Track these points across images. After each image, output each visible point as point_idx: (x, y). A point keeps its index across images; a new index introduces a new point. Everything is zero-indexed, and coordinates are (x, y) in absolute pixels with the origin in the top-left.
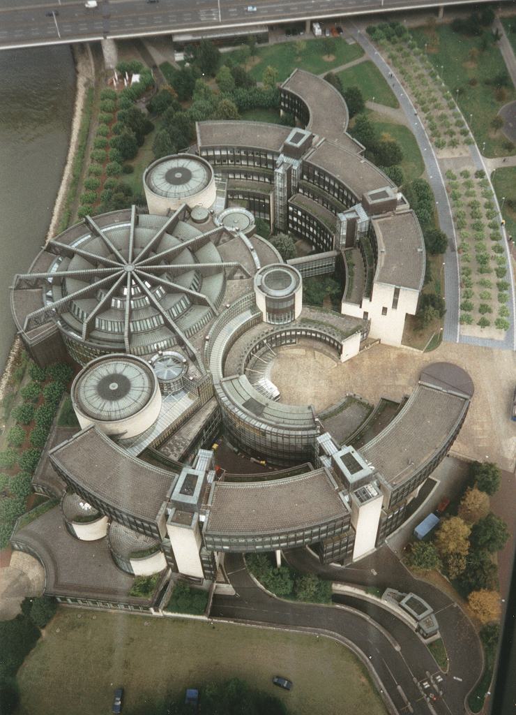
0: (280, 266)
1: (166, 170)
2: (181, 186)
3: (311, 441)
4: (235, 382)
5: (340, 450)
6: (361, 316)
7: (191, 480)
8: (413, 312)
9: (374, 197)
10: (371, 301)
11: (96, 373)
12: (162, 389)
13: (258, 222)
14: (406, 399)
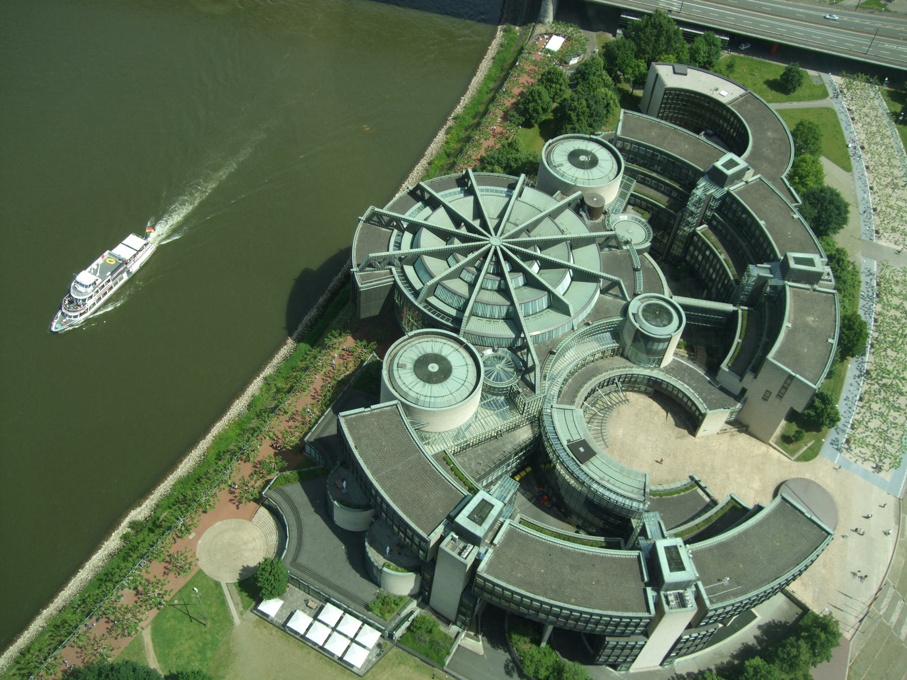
1: (572, 149)
2: (582, 171)
4: (568, 413)
5: (664, 537)
7: (484, 508)
9: (798, 261)
10: (755, 377)
13: (654, 240)
14: (759, 508)
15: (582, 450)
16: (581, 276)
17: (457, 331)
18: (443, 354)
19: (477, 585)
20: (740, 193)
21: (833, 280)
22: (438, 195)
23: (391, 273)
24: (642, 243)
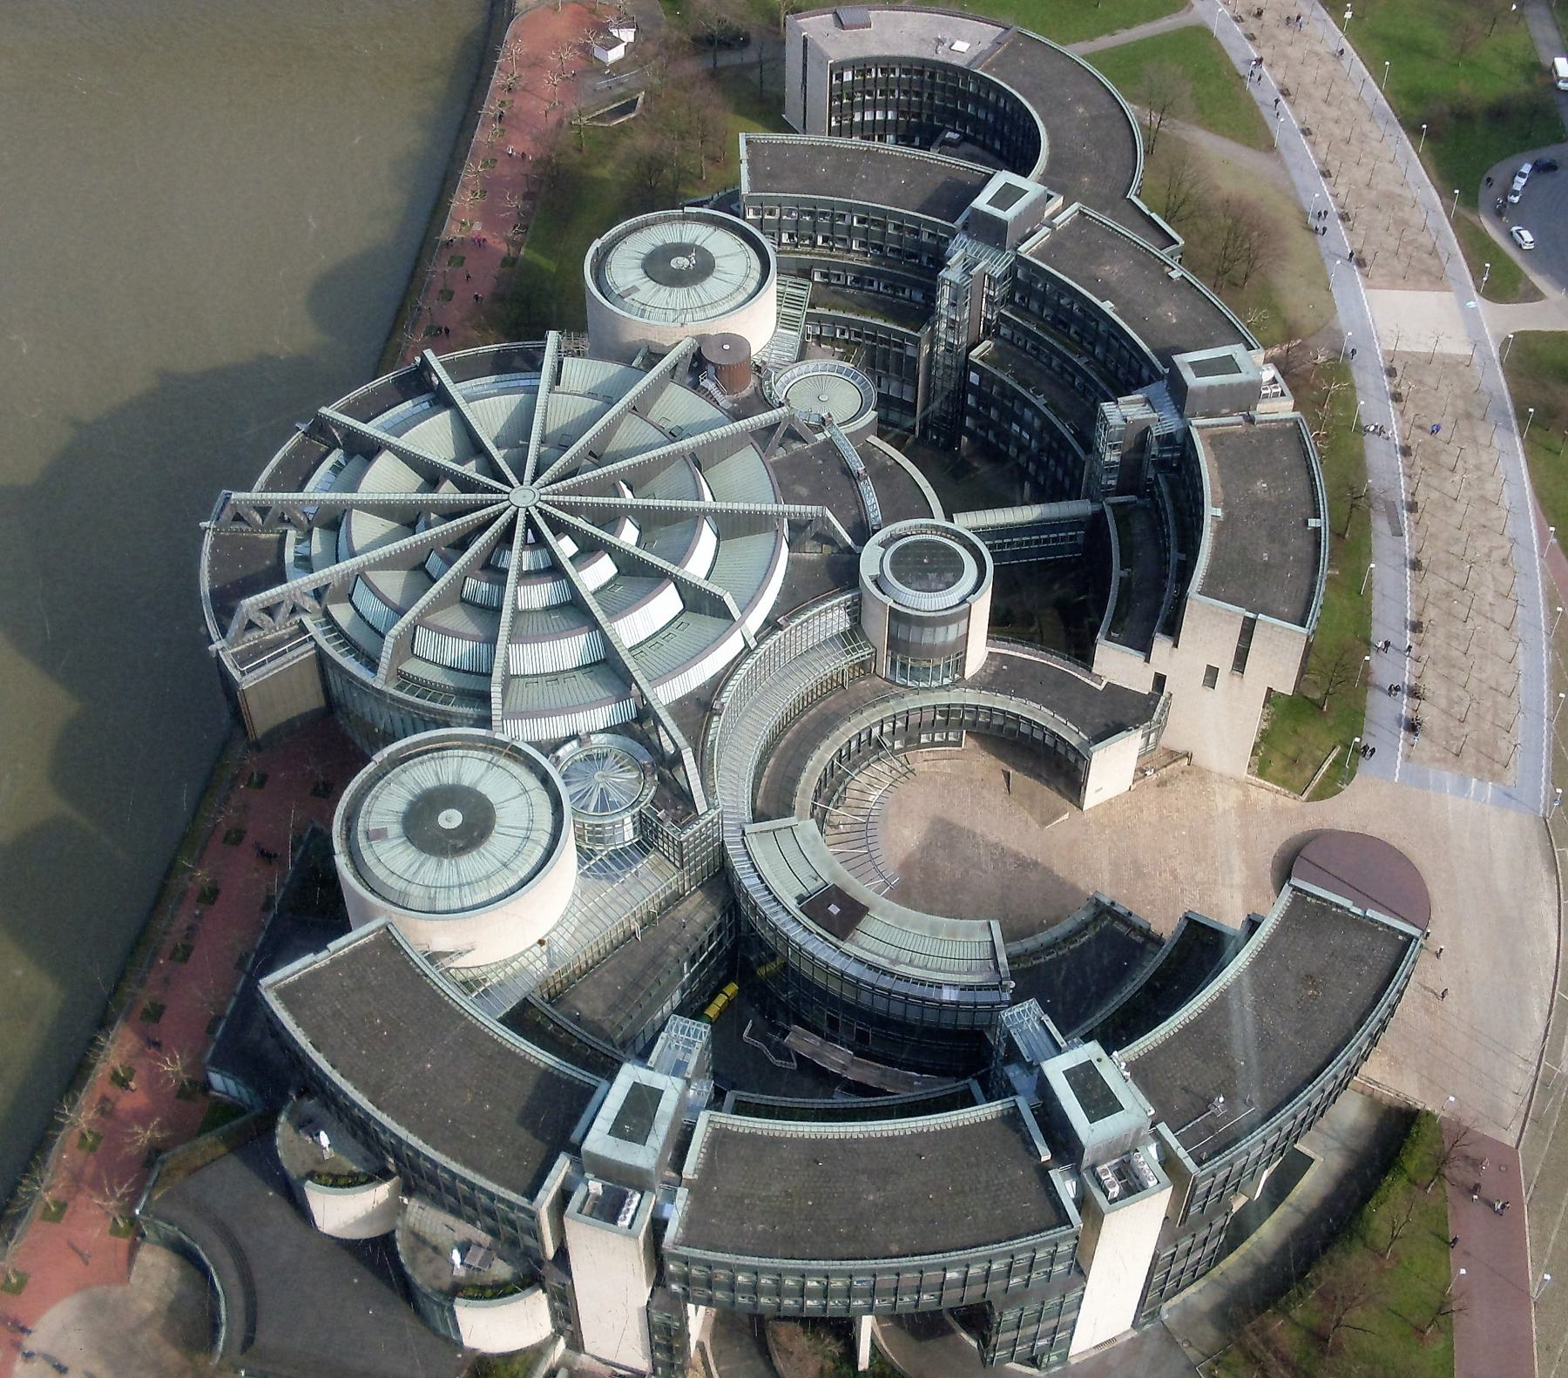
0: (937, 528)
1: (647, 249)
3: (981, 1020)
4: (785, 837)
6: (1145, 687)
7: (642, 1102)
8: (1286, 687)
9: (1201, 368)
10: (1176, 645)
11: (404, 777)
12: (578, 837)
13: (884, 402)
14: (1253, 925)
15: (834, 909)
16: (732, 526)
17: (486, 722)
18: (466, 782)
19: (673, 1278)
20: (1041, 254)
21: (1287, 391)
22: (370, 429)
23: (303, 629)
24: (854, 418)
